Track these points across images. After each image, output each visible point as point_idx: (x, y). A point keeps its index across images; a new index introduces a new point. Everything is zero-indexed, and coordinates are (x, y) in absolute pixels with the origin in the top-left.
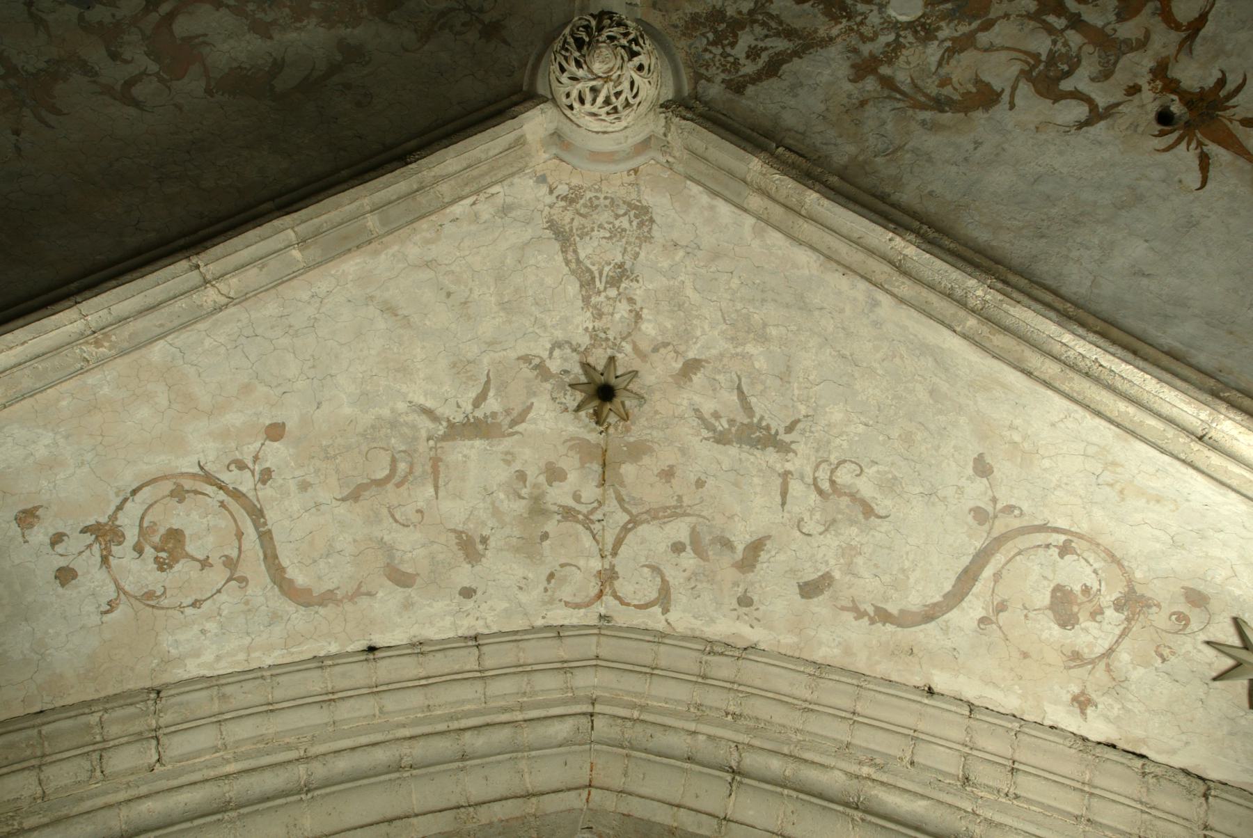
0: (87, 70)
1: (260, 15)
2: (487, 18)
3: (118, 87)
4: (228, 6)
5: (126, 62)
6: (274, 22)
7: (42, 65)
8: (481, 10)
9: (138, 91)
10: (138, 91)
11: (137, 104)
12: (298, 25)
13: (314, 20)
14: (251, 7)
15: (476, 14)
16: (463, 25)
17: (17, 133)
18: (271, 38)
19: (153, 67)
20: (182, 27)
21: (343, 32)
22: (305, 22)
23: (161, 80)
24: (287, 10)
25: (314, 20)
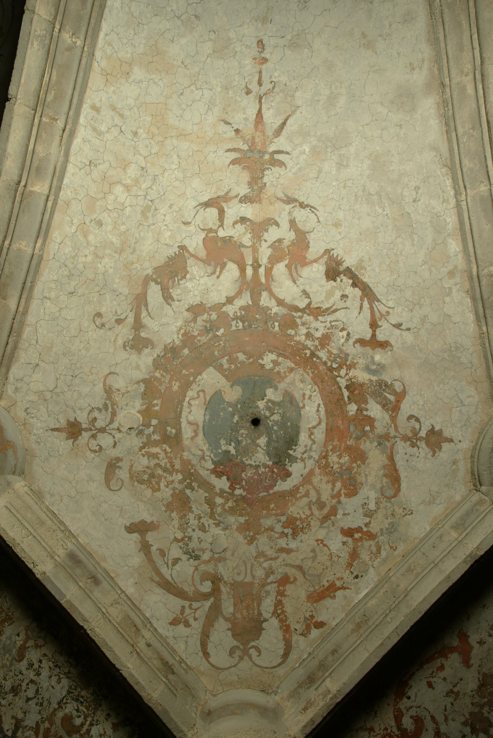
0: (245, 199)
1: (205, 316)
2: (85, 435)
3: (224, 205)
4: (224, 305)
5: (235, 223)
6: (195, 320)
7: (265, 180)
8: (94, 436)
9: (213, 212)
10: (213, 212)
11: (207, 204)
12: (182, 331)
13: (177, 342)
14: (214, 316)
15: (94, 432)
16: (95, 419)
17: (237, 131)
18: (188, 310)
19: (221, 233)
20: (232, 270)
21: (158, 351)
22: (180, 336)
23: (210, 230)
24: (196, 334)
25: (177, 342)
